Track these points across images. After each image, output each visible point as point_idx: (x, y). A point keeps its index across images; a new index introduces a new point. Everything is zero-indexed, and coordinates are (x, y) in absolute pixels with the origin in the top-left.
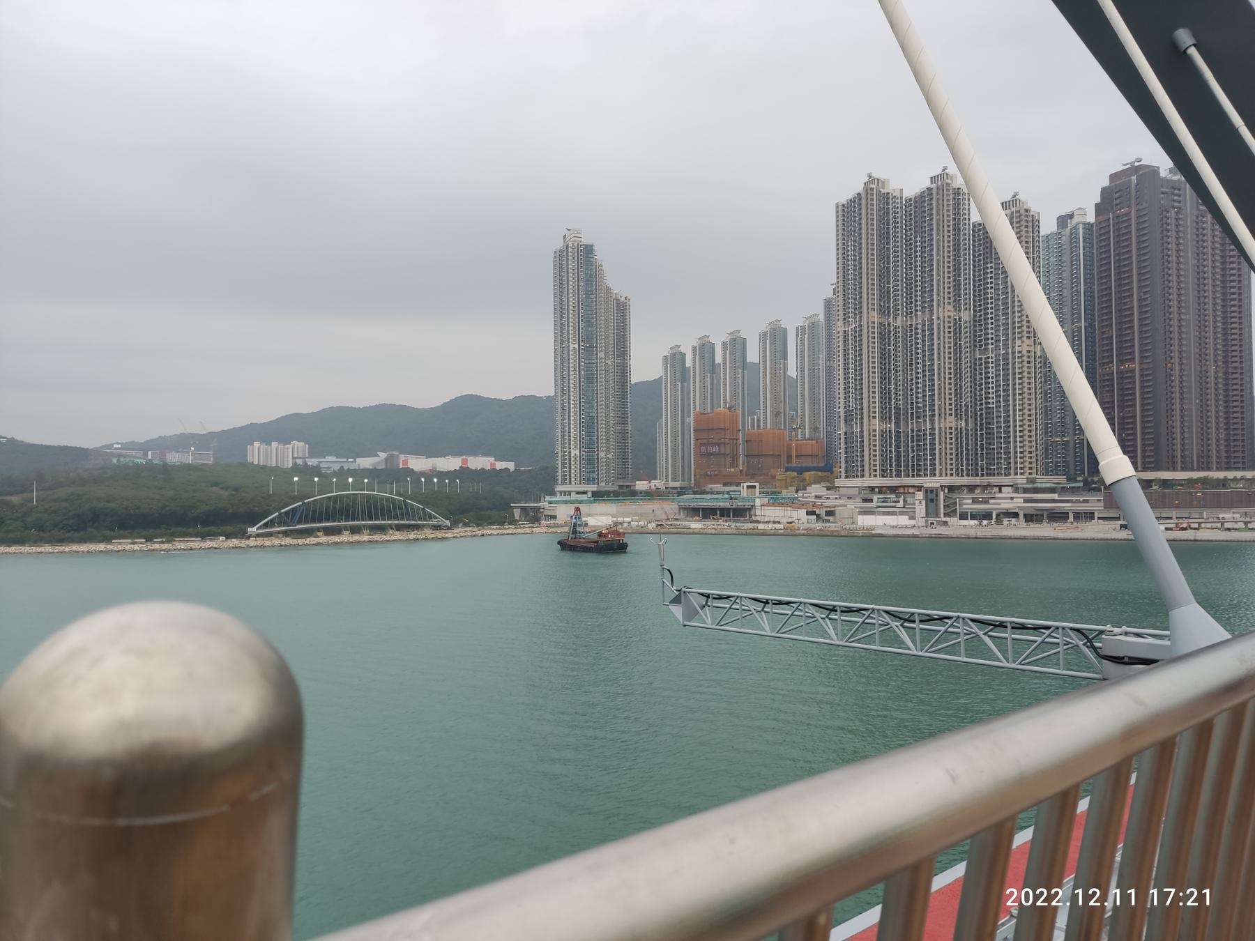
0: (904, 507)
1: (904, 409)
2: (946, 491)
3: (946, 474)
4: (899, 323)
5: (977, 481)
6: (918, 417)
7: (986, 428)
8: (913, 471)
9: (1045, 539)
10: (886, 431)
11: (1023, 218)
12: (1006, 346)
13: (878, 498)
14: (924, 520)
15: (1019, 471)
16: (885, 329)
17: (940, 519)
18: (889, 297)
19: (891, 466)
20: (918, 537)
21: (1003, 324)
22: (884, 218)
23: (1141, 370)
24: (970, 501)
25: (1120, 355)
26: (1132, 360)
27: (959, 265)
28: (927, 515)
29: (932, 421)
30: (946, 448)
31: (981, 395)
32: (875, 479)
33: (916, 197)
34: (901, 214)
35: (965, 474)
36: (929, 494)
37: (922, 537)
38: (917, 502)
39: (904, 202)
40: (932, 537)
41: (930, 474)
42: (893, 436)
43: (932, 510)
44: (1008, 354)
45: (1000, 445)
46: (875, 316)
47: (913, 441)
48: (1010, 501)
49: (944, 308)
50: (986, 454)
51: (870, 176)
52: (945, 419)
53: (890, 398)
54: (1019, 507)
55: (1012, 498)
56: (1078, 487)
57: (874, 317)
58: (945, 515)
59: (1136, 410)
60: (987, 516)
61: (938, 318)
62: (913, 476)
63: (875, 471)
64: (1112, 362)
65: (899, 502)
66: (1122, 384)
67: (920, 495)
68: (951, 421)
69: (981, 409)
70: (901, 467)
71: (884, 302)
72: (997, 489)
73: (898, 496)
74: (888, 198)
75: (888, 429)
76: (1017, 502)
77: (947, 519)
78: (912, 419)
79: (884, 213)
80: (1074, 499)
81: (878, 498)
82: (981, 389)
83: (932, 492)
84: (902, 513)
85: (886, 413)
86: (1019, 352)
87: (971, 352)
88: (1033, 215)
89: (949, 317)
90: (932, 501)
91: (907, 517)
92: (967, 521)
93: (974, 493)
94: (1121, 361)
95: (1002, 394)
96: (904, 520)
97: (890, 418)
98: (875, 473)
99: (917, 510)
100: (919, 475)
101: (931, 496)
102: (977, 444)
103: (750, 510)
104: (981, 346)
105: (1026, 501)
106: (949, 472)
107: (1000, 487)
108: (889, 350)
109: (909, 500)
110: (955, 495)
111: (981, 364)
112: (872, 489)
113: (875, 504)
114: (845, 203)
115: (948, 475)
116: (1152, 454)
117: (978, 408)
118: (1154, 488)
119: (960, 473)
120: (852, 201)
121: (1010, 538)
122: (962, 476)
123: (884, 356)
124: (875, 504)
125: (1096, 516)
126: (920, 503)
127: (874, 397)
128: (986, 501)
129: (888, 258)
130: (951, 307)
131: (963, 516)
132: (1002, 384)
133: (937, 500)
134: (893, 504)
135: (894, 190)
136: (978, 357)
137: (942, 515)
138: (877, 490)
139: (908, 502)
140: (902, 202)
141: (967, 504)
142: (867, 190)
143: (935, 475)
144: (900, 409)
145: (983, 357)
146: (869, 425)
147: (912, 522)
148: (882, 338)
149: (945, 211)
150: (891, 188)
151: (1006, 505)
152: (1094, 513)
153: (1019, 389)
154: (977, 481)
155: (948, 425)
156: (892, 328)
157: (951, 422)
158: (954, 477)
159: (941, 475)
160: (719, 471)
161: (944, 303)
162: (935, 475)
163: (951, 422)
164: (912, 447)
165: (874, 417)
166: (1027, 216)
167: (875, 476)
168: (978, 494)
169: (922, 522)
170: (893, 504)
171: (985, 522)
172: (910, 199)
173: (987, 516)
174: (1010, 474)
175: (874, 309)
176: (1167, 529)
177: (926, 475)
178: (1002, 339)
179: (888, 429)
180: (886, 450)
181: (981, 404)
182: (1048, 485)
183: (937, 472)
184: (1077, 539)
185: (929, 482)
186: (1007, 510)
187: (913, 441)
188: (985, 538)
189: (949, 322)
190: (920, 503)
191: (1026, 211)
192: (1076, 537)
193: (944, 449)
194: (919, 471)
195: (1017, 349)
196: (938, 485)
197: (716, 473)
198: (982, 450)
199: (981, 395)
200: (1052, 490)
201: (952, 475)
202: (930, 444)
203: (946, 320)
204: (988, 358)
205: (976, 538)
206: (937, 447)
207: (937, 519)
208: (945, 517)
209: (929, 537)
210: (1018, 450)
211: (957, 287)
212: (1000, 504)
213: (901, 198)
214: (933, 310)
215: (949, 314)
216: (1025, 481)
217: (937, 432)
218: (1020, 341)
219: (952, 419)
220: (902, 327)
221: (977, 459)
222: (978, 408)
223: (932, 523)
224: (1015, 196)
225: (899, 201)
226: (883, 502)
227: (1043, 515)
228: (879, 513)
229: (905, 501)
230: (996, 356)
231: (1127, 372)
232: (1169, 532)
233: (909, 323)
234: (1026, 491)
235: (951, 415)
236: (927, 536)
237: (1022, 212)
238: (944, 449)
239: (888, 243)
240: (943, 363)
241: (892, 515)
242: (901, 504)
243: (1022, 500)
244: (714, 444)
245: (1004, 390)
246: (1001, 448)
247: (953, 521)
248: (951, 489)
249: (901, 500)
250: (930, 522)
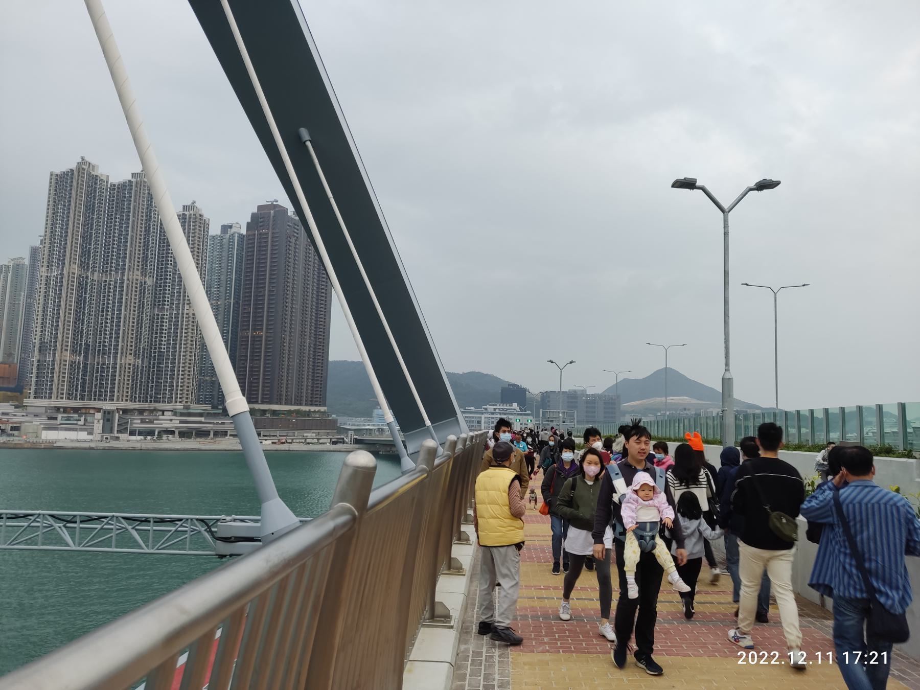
0: (84, 425)
1: (92, 346)
2: (121, 413)
3: (122, 400)
4: (96, 278)
5: (146, 406)
6: (104, 354)
7: (157, 367)
8: (95, 396)
9: (192, 450)
10: (75, 362)
11: (198, 220)
12: (178, 308)
13: (62, 417)
14: (100, 435)
15: (178, 400)
16: (83, 280)
17: (113, 435)
18: (89, 256)
19: (77, 391)
20: (94, 449)
21: (177, 292)
22: (91, 194)
23: (267, 337)
24: (139, 421)
25: (254, 325)
26: (261, 329)
27: (148, 243)
28: (103, 431)
29: (115, 358)
30: (124, 380)
31: (156, 341)
32: (62, 400)
33: (119, 185)
34: (106, 194)
35: (137, 401)
36: (106, 415)
37: (97, 449)
38: (96, 421)
39: (109, 186)
40: (105, 449)
41: (109, 399)
42: (81, 367)
44: (179, 314)
45: (166, 380)
46: (76, 269)
47: (97, 372)
48: (169, 422)
49: (133, 272)
50: (156, 386)
51: (83, 159)
52: (126, 357)
53: (82, 336)
54: (176, 427)
55: (171, 420)
56: (219, 413)
57: (75, 269)
58: (118, 432)
59: (260, 363)
60: (151, 433)
61: (128, 280)
62: (95, 400)
63: (63, 394)
64: (249, 329)
65: (80, 420)
66: (253, 344)
67: (99, 415)
68: (130, 359)
69: (155, 352)
70: (85, 392)
71: (85, 259)
72: (161, 413)
73: (80, 416)
74: (97, 180)
75: (77, 361)
76: (174, 423)
77: (120, 435)
78: (99, 354)
79: (91, 190)
80: (215, 421)
81: (62, 417)
82: (156, 337)
83: (109, 413)
84: (82, 430)
85: (77, 347)
86: (187, 314)
87: (151, 309)
88: (205, 220)
89: (137, 280)
90: (108, 420)
91: (86, 433)
92: (135, 437)
93: (143, 415)
94: (254, 330)
95: (172, 343)
96: (83, 435)
97: (80, 352)
98: (62, 396)
99: (95, 428)
100: (99, 400)
101: (108, 416)
102: (149, 378)
104: (159, 305)
105: (181, 422)
106: (124, 398)
107: (163, 411)
108: (85, 297)
109: (89, 419)
110: (128, 416)
111: (158, 319)
112: (58, 409)
113: (59, 422)
114: (59, 173)
115: (124, 400)
116: (268, 393)
117: (153, 351)
118: (267, 415)
119: (133, 399)
120: (65, 174)
121: (167, 450)
122: (135, 402)
123: (80, 302)
124: (59, 422)
125: (229, 434)
126: (98, 421)
127: (68, 334)
128: (151, 422)
129: (92, 225)
130: (139, 273)
131: (132, 433)
132: (172, 335)
133: (112, 420)
134: (75, 422)
135: (102, 175)
136: (156, 313)
137: (116, 432)
138: (62, 410)
139: (88, 421)
140: (107, 186)
141: (137, 424)
142: (79, 169)
143: (113, 400)
144: (89, 345)
145: (160, 314)
146: (61, 356)
147: (90, 437)
148: (80, 286)
149: (141, 201)
150: (99, 172)
151: (167, 425)
152: (227, 432)
153: (184, 340)
154: (146, 406)
155: (128, 362)
156: (89, 280)
157: (130, 360)
158: (128, 402)
159: (118, 400)
161: (134, 269)
162: (113, 400)
163: (130, 360)
164: (97, 377)
165: (66, 350)
166: (201, 219)
167: (62, 398)
168: (146, 416)
169: (98, 437)
170: (75, 422)
171: (149, 438)
172: (114, 185)
173: (151, 433)
174: (171, 402)
175: (76, 263)
176: (273, 443)
177: (105, 400)
178: (175, 302)
179: (77, 361)
180: (74, 378)
181: (155, 348)
182: (199, 411)
183: (115, 398)
184: (214, 450)
185: (107, 405)
186: (167, 428)
187: (97, 372)
188: (148, 450)
189: (137, 284)
190: (98, 421)
191: (201, 215)
192: (213, 449)
193: (123, 380)
194: (100, 397)
195: (185, 312)
196: (114, 408)
198: (153, 382)
199: (156, 341)
200: (201, 415)
201: (127, 400)
202: (111, 375)
203: (134, 281)
204: (164, 315)
205: (141, 450)
206: (117, 378)
207: (111, 435)
208: (117, 433)
209: (102, 449)
210: (180, 384)
211: (145, 259)
212: (162, 424)
213: (107, 182)
214: (125, 272)
215: (137, 277)
216: (182, 407)
217: (118, 366)
218: (188, 306)
219: (132, 357)
220: (98, 281)
221: (148, 390)
222: (153, 351)
223: (107, 438)
224: (193, 204)
225: (105, 184)
226: (66, 420)
227: (192, 433)
228: (62, 429)
229: (86, 420)
230: (170, 314)
231: (257, 337)
232: (274, 445)
233: (104, 279)
234: (182, 414)
235: (131, 354)
236: (101, 448)
237: (198, 216)
238: (123, 380)
239: (93, 214)
240: (128, 314)
241: (73, 430)
242: (82, 422)
243: (178, 421)
245: (173, 340)
246: (167, 382)
247: (124, 436)
248: (125, 411)
249: (83, 419)
250: (105, 437)
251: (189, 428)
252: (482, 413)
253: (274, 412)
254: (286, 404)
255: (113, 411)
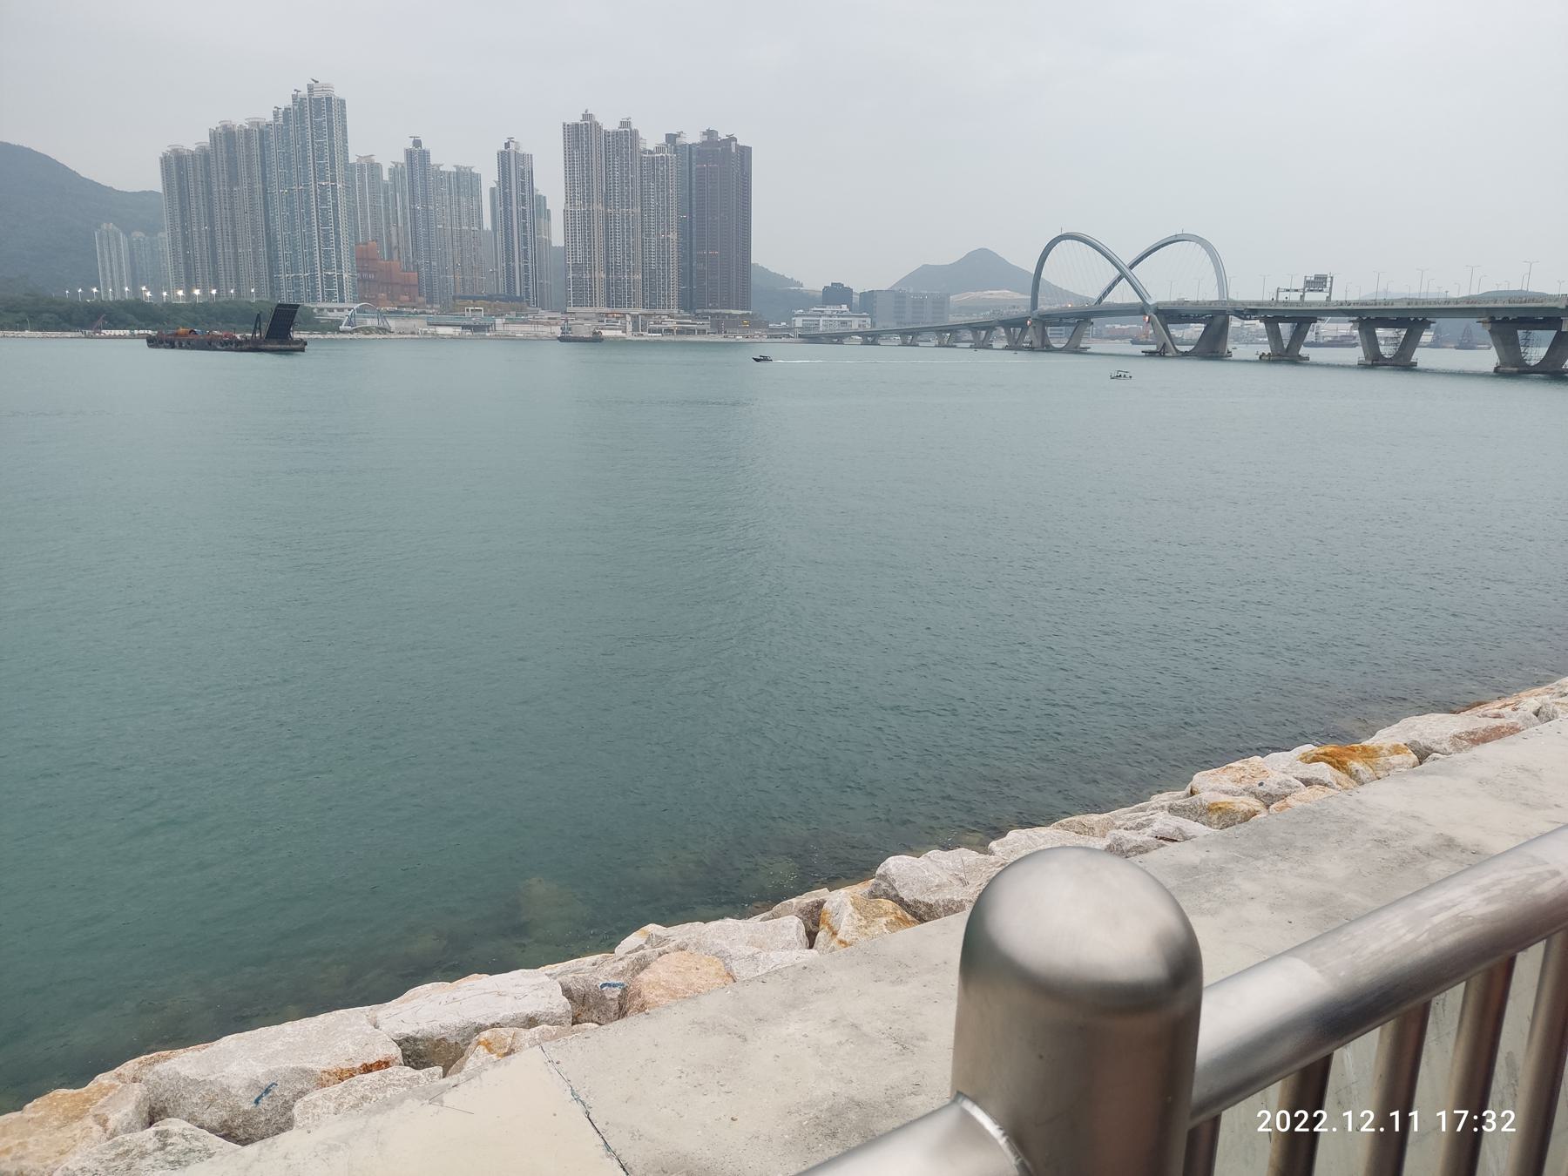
43: (635, 329)
46: (600, 207)
67: (629, 318)
76: (672, 324)
96: (619, 333)
103: (489, 326)
105: (678, 323)
124: (605, 323)
141: (651, 325)
151: (670, 325)
160: (377, 296)
197: (374, 297)
234: (678, 318)
242: (619, 324)
244: (371, 272)
247: (646, 333)
251: (683, 328)
252: (820, 316)
253: (729, 315)
254: (737, 309)
255: (638, 316)
